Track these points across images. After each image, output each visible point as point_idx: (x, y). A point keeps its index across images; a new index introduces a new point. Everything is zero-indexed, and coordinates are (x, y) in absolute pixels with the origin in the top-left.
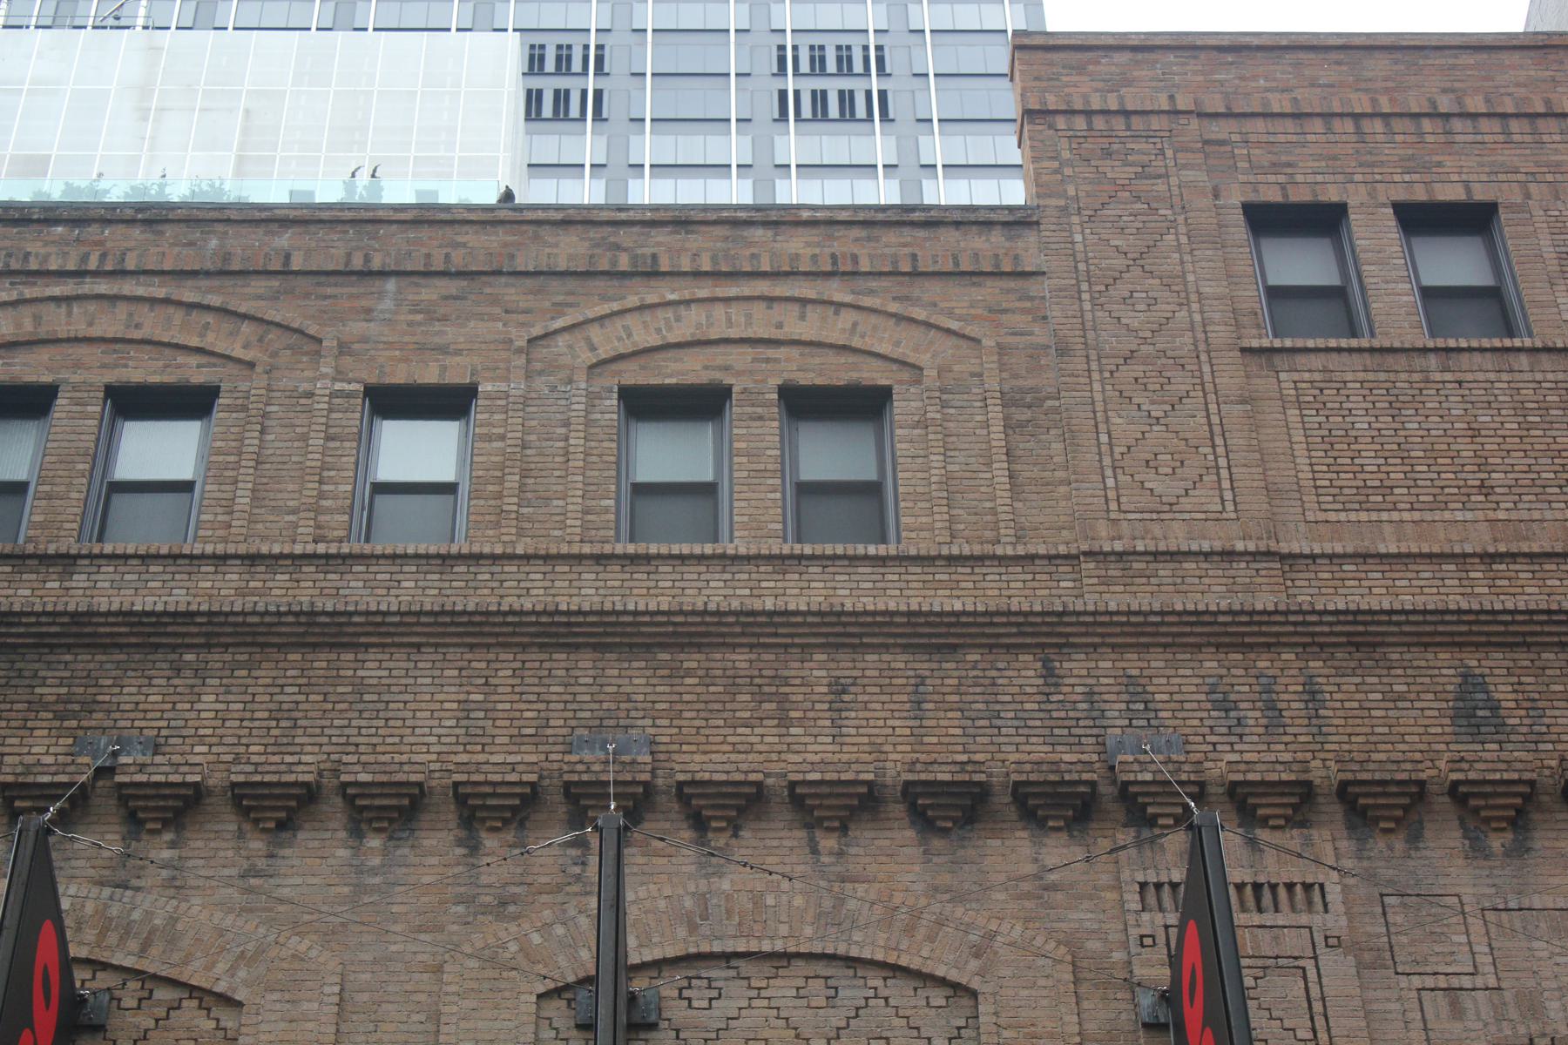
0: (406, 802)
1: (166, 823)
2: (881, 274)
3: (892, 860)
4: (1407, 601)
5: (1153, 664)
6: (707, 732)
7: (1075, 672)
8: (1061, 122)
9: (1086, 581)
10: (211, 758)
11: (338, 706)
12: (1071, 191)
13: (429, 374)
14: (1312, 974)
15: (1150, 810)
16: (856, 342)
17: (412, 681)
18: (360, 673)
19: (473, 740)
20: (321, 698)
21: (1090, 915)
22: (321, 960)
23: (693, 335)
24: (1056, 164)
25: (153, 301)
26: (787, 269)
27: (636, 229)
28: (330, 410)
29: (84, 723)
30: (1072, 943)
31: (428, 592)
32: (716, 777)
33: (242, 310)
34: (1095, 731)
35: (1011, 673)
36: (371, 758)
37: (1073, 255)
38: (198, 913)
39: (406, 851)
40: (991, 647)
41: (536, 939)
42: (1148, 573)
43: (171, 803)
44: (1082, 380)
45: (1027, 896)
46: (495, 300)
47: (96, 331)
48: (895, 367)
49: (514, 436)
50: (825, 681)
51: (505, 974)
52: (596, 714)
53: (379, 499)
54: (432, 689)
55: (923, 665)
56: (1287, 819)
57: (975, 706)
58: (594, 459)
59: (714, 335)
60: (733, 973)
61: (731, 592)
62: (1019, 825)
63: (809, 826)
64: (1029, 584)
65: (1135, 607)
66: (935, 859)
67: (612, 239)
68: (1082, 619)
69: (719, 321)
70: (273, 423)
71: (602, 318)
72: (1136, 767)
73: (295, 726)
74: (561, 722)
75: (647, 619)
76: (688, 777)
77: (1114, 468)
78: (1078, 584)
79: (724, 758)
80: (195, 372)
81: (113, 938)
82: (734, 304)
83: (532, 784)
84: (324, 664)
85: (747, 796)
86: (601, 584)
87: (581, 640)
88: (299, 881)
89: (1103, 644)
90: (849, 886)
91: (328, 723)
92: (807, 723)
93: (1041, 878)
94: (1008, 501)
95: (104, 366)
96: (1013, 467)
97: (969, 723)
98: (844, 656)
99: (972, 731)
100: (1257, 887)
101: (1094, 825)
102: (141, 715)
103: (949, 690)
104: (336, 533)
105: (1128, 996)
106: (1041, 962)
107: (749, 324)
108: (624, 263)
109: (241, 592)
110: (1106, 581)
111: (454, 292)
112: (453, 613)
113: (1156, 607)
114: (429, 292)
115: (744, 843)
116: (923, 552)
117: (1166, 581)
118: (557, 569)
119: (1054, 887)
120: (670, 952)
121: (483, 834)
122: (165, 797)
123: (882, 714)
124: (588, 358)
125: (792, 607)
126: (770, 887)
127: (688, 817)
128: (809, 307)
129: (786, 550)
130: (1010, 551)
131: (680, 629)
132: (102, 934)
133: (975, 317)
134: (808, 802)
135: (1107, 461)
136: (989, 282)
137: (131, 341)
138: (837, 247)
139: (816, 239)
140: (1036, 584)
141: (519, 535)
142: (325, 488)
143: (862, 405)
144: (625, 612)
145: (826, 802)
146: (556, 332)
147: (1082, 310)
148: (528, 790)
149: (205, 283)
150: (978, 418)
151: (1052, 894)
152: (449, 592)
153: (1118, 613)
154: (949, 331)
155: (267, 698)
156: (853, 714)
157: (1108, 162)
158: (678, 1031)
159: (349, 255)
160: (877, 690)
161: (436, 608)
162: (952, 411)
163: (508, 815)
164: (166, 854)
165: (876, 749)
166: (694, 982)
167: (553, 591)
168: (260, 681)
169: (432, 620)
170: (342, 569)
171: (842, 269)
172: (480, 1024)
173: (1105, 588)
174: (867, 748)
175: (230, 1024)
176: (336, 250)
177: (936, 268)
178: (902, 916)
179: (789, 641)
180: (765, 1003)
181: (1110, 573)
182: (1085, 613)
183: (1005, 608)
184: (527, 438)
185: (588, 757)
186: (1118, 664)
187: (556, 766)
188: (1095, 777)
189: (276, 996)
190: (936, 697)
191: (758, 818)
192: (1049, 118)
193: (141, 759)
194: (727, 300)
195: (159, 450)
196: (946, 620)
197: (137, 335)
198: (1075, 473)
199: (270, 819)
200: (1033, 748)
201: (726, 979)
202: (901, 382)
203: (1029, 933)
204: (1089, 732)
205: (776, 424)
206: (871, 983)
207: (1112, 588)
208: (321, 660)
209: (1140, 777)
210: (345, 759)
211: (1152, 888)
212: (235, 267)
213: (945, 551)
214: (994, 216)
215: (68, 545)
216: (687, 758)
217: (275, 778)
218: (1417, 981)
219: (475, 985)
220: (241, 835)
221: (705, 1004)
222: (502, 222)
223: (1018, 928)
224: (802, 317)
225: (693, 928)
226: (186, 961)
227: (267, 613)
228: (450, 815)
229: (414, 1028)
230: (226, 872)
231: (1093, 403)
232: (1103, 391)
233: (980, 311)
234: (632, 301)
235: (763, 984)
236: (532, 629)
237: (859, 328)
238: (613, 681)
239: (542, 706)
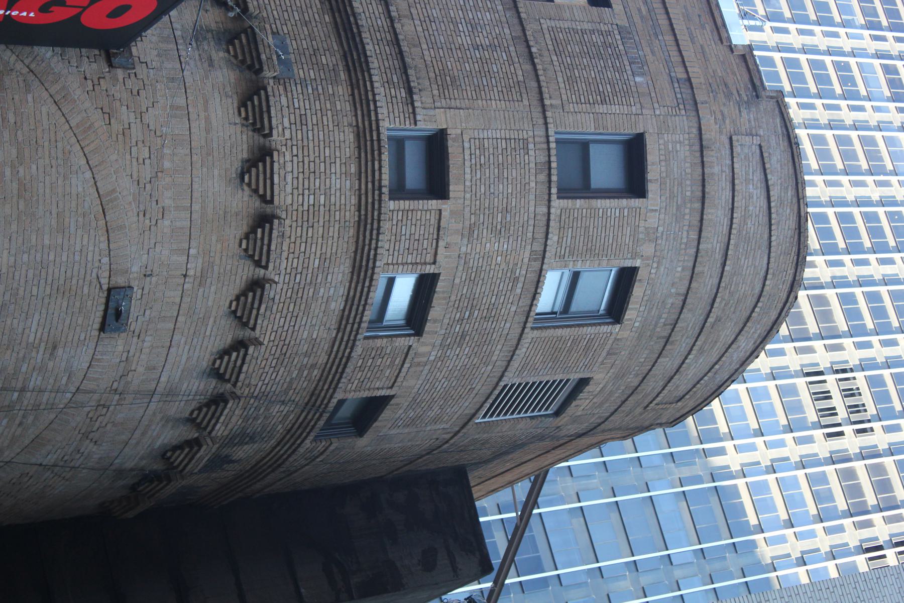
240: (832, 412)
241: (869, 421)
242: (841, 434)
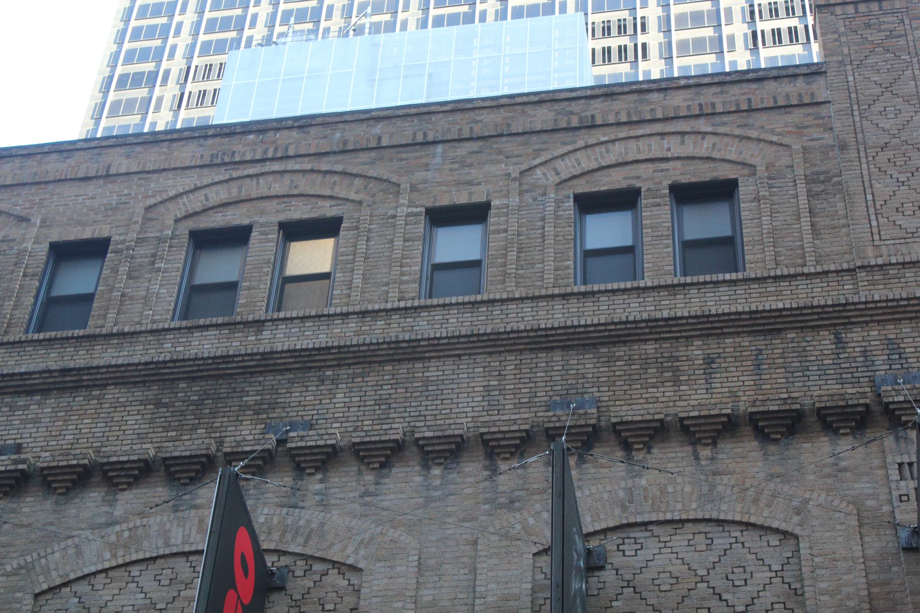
0: (453, 446)
1: (317, 469)
2: (729, 112)
3: (744, 459)
5: (904, 331)
6: (631, 392)
7: (855, 339)
8: (838, 10)
9: (860, 284)
10: (342, 430)
11: (414, 395)
12: (846, 51)
13: (462, 198)
15: (903, 418)
16: (716, 155)
17: (456, 376)
18: (426, 374)
19: (492, 408)
20: (404, 390)
21: (868, 485)
22: (407, 541)
23: (617, 160)
24: (836, 36)
25: (304, 172)
26: (673, 115)
27: (582, 101)
28: (406, 224)
29: (271, 415)
30: (857, 503)
31: (464, 324)
32: (635, 418)
33: (355, 172)
34: (868, 374)
35: (815, 343)
36: (432, 423)
37: (848, 89)
38: (335, 518)
39: (455, 475)
40: (802, 328)
41: (531, 521)
42: (899, 276)
43: (319, 457)
44: (855, 163)
45: (829, 476)
46: (500, 152)
47: (273, 192)
48: (739, 167)
49: (513, 229)
50: (701, 357)
51: (514, 543)
52: (564, 387)
53: (436, 274)
54: (468, 380)
57: (793, 364)
58: (560, 238)
59: (630, 158)
60: (649, 534)
61: (643, 309)
62: (823, 434)
64: (825, 289)
65: (891, 297)
66: (771, 458)
67: (568, 109)
68: (858, 307)
69: (632, 150)
70: (374, 235)
71: (563, 155)
72: (893, 393)
73: (390, 408)
74: (544, 394)
75: (592, 329)
76: (619, 420)
77: (876, 214)
78: (855, 286)
79: (639, 407)
80: (328, 210)
81: (289, 536)
82: (641, 139)
83: (526, 431)
84: (405, 371)
85: (655, 429)
86: (566, 311)
87: (554, 344)
88: (393, 497)
89: (872, 321)
90: (717, 477)
91: (408, 404)
92: (690, 382)
93: (837, 465)
94: (811, 240)
95: (277, 211)
96: (813, 219)
97: (790, 375)
98: (712, 342)
99: (791, 380)
101: (869, 430)
102: (302, 408)
103: (777, 356)
104: (411, 295)
105: (893, 532)
106: (837, 515)
107: (650, 150)
108: (575, 122)
109: (357, 334)
110: (873, 283)
111: (476, 149)
112: (478, 335)
113: (904, 295)
114: (463, 150)
115: (654, 456)
116: (759, 275)
117: (910, 279)
118: (540, 304)
120: (611, 524)
121: (499, 462)
122: (315, 454)
123: (737, 374)
124: (553, 179)
125: (679, 314)
126: (672, 479)
127: (620, 444)
128: (686, 137)
129: (676, 281)
130: (812, 270)
131: (613, 333)
132: (283, 535)
133: (789, 133)
134: (692, 429)
135: (872, 210)
136: (796, 110)
137: (293, 196)
138: (702, 100)
139: (690, 96)
140: (829, 289)
141: (517, 286)
142: (404, 269)
143: (722, 191)
144: (579, 326)
145: (703, 428)
146: (536, 166)
147: (854, 121)
148: (524, 434)
149: (332, 158)
150: (791, 192)
151: (844, 473)
152: (476, 323)
153: (880, 301)
154: (771, 142)
155: (373, 393)
156: (718, 375)
157: (869, 31)
158: (617, 570)
159: (415, 134)
160: (733, 359)
161: (469, 333)
162: (775, 190)
163: (513, 450)
164: (318, 487)
165: (733, 395)
166: (626, 540)
167: (537, 318)
168: (369, 384)
169: (466, 340)
170: (414, 315)
171: (705, 112)
172: (500, 573)
173: (873, 287)
174: (728, 395)
175: (356, 582)
176: (406, 132)
177: (764, 106)
178: (751, 493)
179: (678, 335)
180: (669, 550)
181: (875, 278)
182: (860, 303)
183: (810, 304)
184: (520, 229)
185: (559, 412)
186: (881, 332)
187: (541, 419)
188: (868, 401)
189: (382, 564)
190: (769, 361)
191: (662, 441)
192: (831, 9)
193: (302, 433)
195: (312, 256)
196: (773, 314)
197: (296, 192)
198: (852, 220)
199: (376, 462)
200: (830, 387)
201: (645, 538)
202: (743, 176)
203: (830, 498)
204: (864, 374)
205: (668, 207)
206: (733, 534)
207: (876, 287)
208: (403, 368)
209: (896, 399)
210: (418, 424)
211: (906, 466)
212: (350, 147)
213: (772, 274)
214: (797, 71)
215: (261, 315)
216: (618, 408)
217: (377, 438)
219: (496, 551)
220: (360, 472)
221: (633, 553)
222: (503, 106)
223: (823, 496)
224: (682, 143)
225: (624, 509)
226: (329, 547)
227: (371, 344)
228: (481, 454)
229: (461, 578)
230: (352, 495)
231: (862, 177)
232: (869, 169)
233: (790, 129)
234: (581, 143)
235: (668, 539)
236: (525, 341)
237: (717, 146)
238: (574, 367)
239: (532, 385)
240: (622, 50)
241: (635, 19)
242: (644, 46)
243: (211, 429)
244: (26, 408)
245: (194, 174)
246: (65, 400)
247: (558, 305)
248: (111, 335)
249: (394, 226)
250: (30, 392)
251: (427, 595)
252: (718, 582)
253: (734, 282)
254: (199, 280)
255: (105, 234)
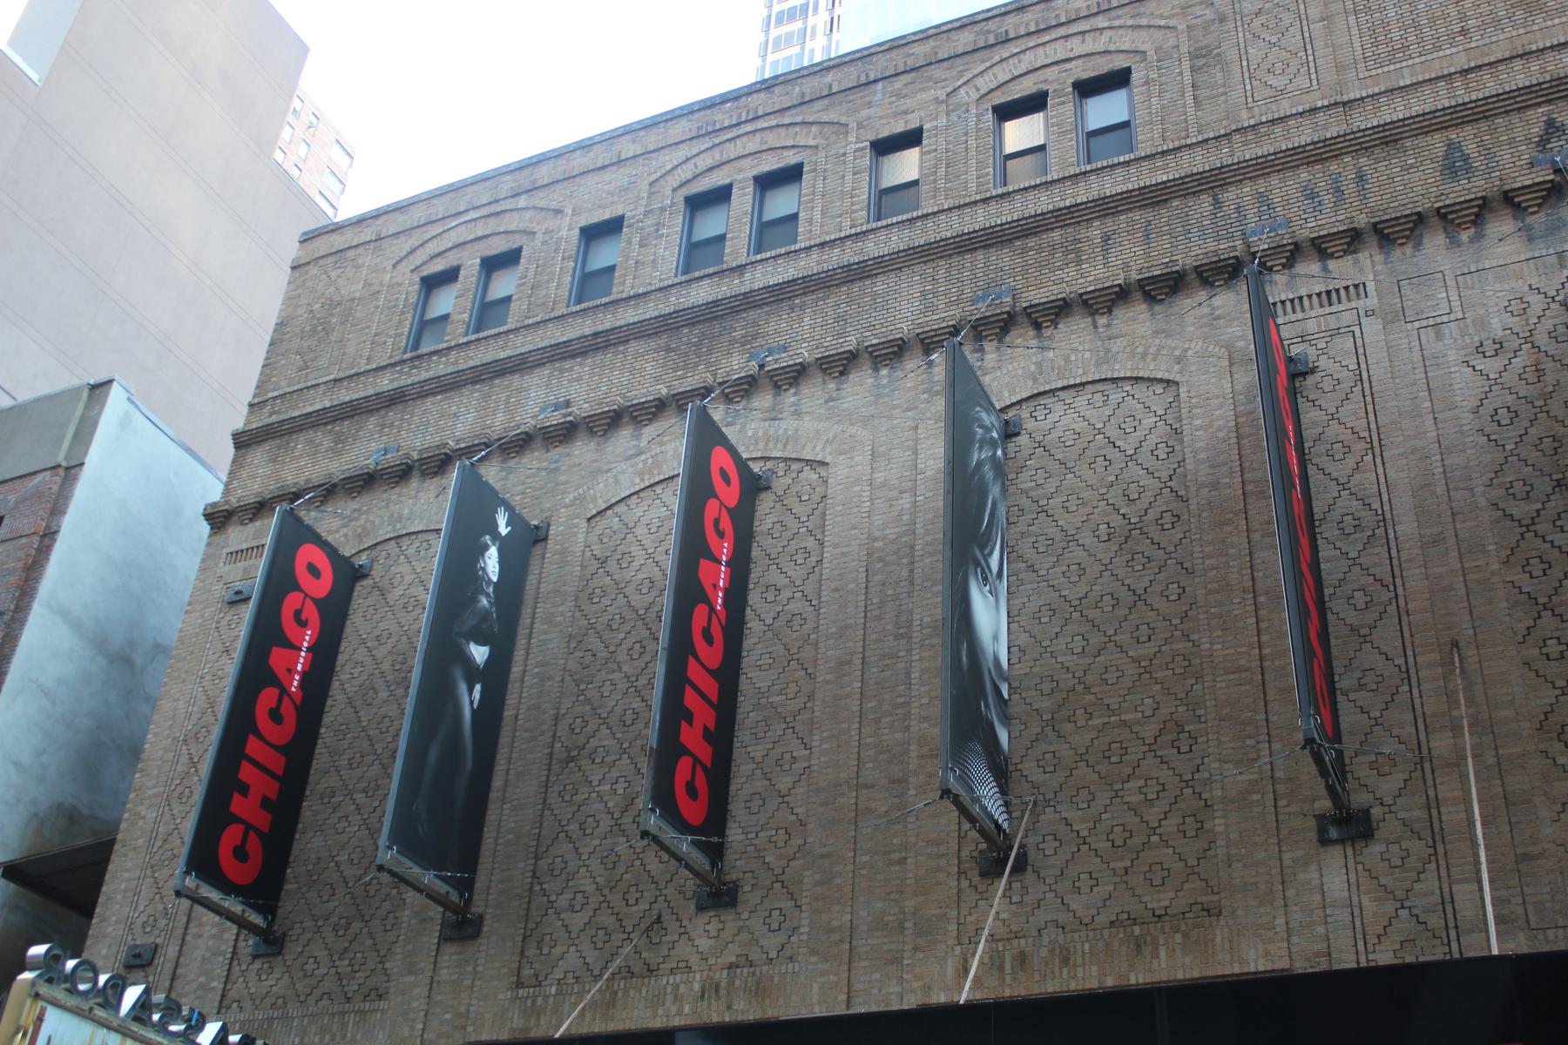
1: (791, 385)
3: (1135, 320)
4: (1416, 110)
13: (899, 127)
14: (1358, 334)
16: (1112, 48)
25: (771, 128)
30: (1228, 346)
38: (807, 424)
45: (1205, 325)
46: (930, 79)
55: (1149, 214)
56: (1345, 251)
63: (1092, 315)
80: (791, 158)
81: (771, 445)
85: (1059, 307)
98: (1108, 220)
100: (1328, 293)
108: (992, 40)
114: (898, 84)
119: (1219, 318)
124: (975, 95)
126: (1076, 347)
135: (1246, 75)
149: (793, 111)
165: (1126, 266)
176: (852, 76)
194: (1044, 44)
208: (856, 287)
215: (743, 260)
218: (1417, 325)
220: (824, 382)
225: (1035, 380)
228: (919, 350)
234: (997, 58)
243: (709, 364)
244: (571, 369)
245: (684, 147)
246: (599, 357)
247: (980, 210)
248: (630, 298)
249: (844, 162)
250: (573, 356)
251: (879, 477)
252: (1112, 432)
253: (1127, 163)
254: (767, 217)
255: (620, 213)
